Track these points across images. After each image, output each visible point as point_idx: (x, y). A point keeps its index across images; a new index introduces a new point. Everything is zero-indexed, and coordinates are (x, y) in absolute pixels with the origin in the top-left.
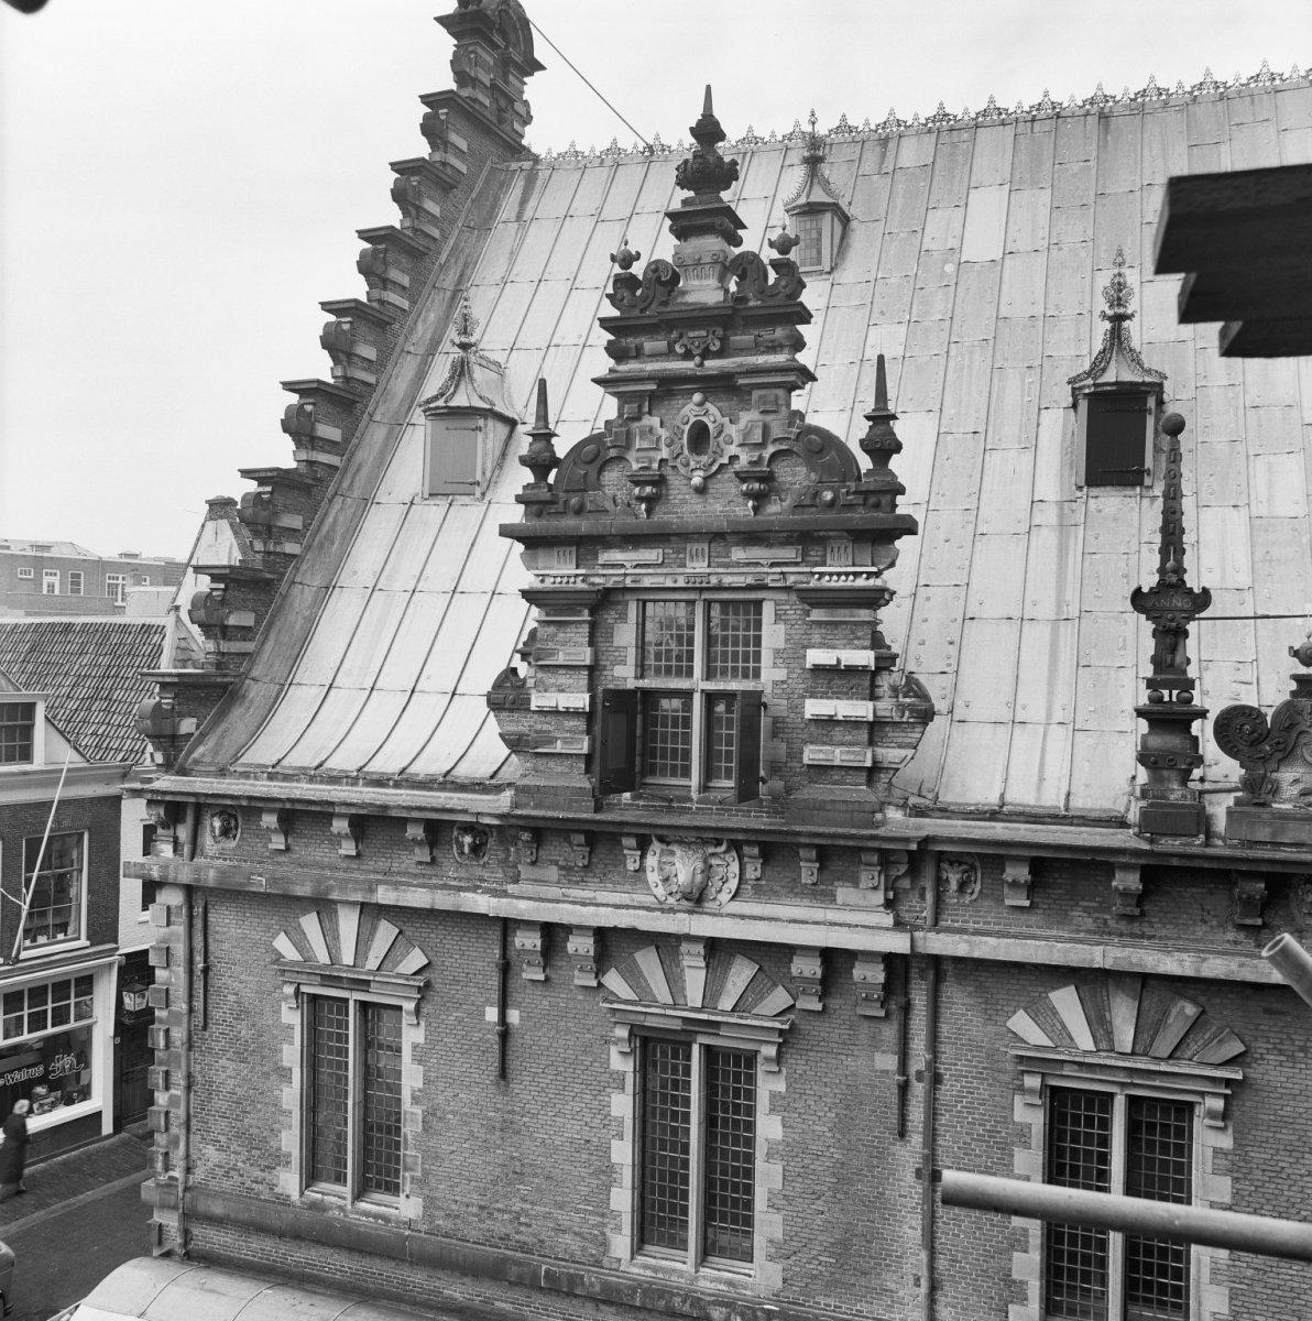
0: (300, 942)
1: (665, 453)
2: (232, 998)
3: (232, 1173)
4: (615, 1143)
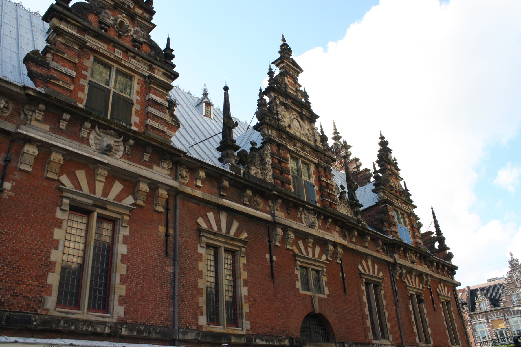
1: (111, 22)
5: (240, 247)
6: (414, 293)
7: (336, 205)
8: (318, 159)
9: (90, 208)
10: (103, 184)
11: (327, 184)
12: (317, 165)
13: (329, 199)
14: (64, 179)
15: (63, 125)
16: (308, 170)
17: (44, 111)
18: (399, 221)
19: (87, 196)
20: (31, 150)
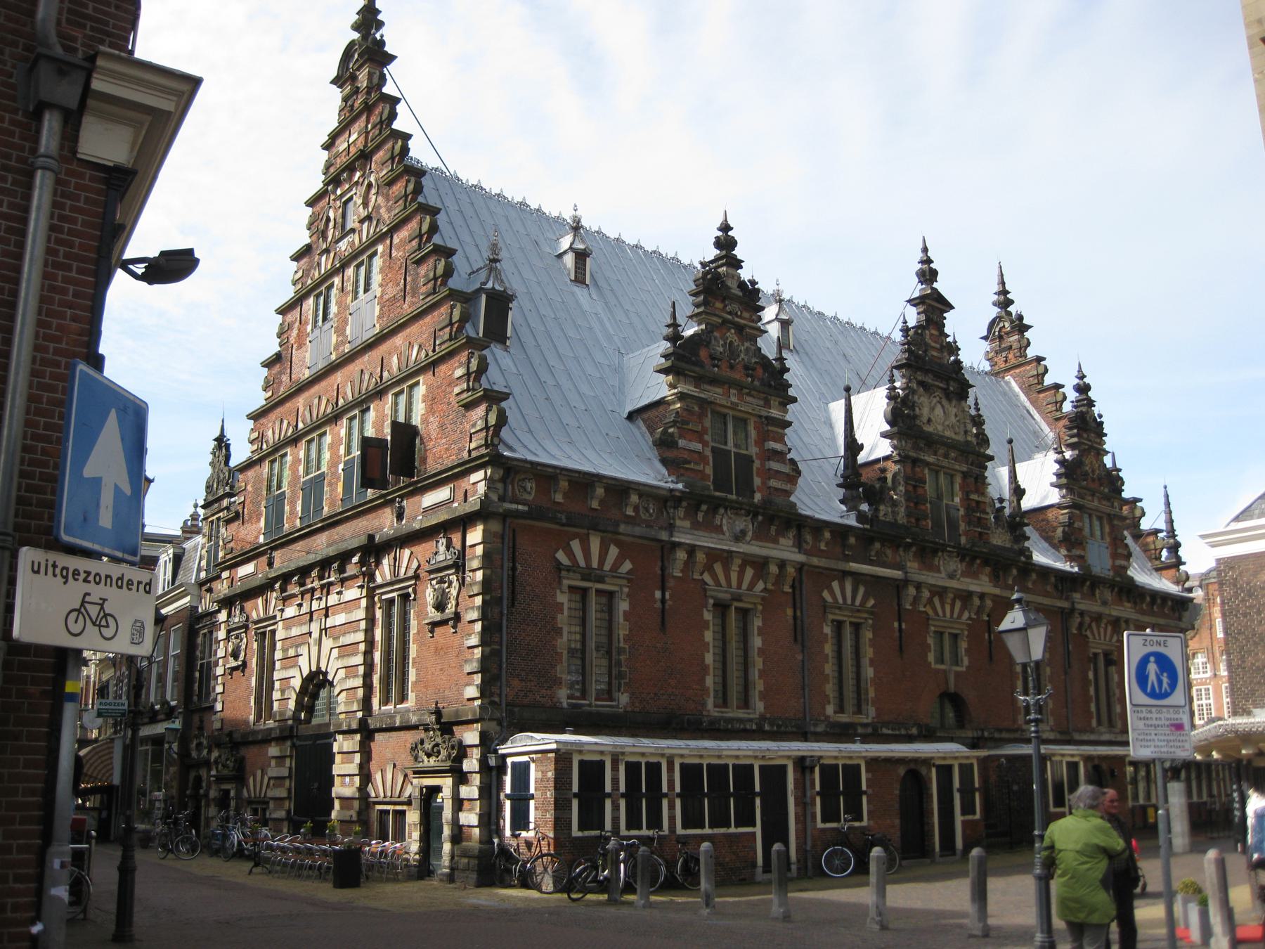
0: (570, 554)
2: (528, 588)
5: (866, 619)
6: (1100, 651)
7: (987, 534)
8: (967, 464)
11: (978, 502)
12: (965, 475)
13: (978, 527)
14: (707, 577)
15: (700, 517)
16: (952, 483)
17: (685, 508)
18: (1092, 535)
19: (726, 592)
20: (681, 555)
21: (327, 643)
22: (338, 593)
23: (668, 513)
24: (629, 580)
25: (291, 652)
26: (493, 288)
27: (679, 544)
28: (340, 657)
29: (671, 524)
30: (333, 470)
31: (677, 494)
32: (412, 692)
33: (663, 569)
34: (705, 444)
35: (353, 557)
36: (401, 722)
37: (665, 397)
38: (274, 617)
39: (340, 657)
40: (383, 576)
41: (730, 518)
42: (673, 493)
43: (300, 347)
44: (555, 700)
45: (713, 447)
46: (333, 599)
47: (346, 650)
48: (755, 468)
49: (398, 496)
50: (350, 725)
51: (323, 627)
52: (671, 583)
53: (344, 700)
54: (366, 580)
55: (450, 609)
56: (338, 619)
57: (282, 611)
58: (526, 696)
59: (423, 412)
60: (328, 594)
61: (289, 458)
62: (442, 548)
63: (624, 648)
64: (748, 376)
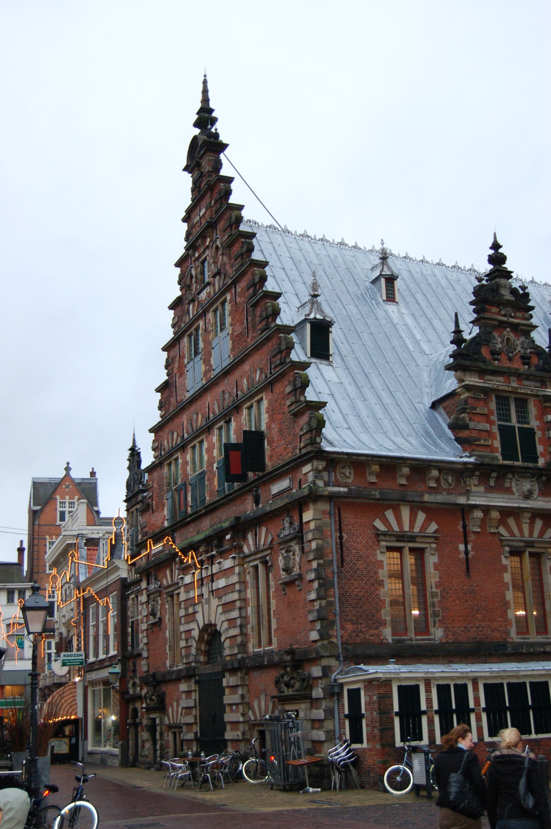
0: (386, 521)
3: (359, 634)
4: (507, 592)
9: (522, 549)
10: (528, 525)
14: (502, 530)
15: (492, 483)
17: (478, 476)
19: (520, 541)
21: (215, 602)
22: (219, 563)
23: (465, 482)
24: (436, 538)
25: (191, 610)
26: (315, 318)
27: (476, 507)
28: (224, 612)
29: (468, 490)
30: (210, 468)
31: (470, 466)
32: (275, 637)
33: (464, 527)
34: (492, 423)
35: (227, 535)
36: (268, 662)
37: (456, 390)
38: (178, 583)
39: (224, 612)
40: (249, 548)
41: (518, 481)
42: (467, 466)
43: (180, 376)
44: (382, 637)
45: (499, 425)
46: (215, 568)
47: (228, 607)
48: (537, 439)
49: (254, 487)
50: (232, 665)
51: (211, 590)
52: (472, 538)
53: (228, 645)
54: (237, 552)
55: (296, 570)
56: (221, 583)
57: (182, 578)
58: (358, 636)
59: (267, 421)
60: (212, 564)
61: (180, 461)
62: (287, 525)
63: (436, 592)
64: (524, 364)
